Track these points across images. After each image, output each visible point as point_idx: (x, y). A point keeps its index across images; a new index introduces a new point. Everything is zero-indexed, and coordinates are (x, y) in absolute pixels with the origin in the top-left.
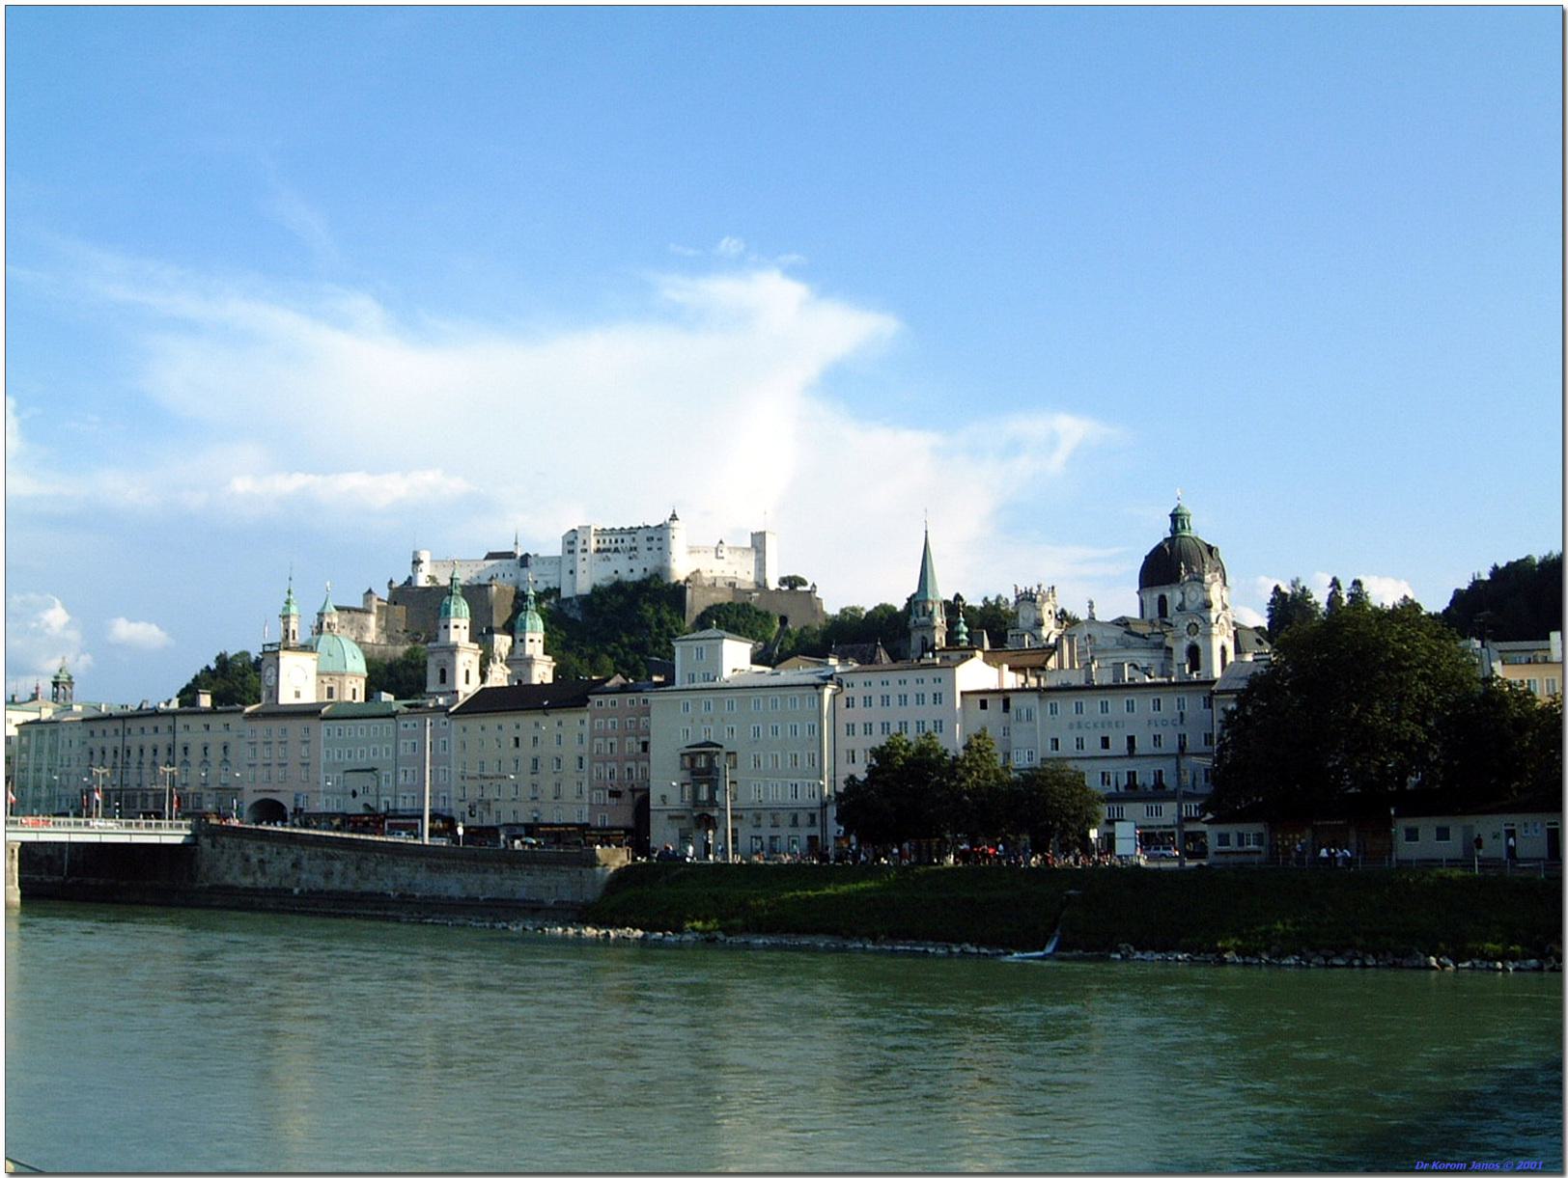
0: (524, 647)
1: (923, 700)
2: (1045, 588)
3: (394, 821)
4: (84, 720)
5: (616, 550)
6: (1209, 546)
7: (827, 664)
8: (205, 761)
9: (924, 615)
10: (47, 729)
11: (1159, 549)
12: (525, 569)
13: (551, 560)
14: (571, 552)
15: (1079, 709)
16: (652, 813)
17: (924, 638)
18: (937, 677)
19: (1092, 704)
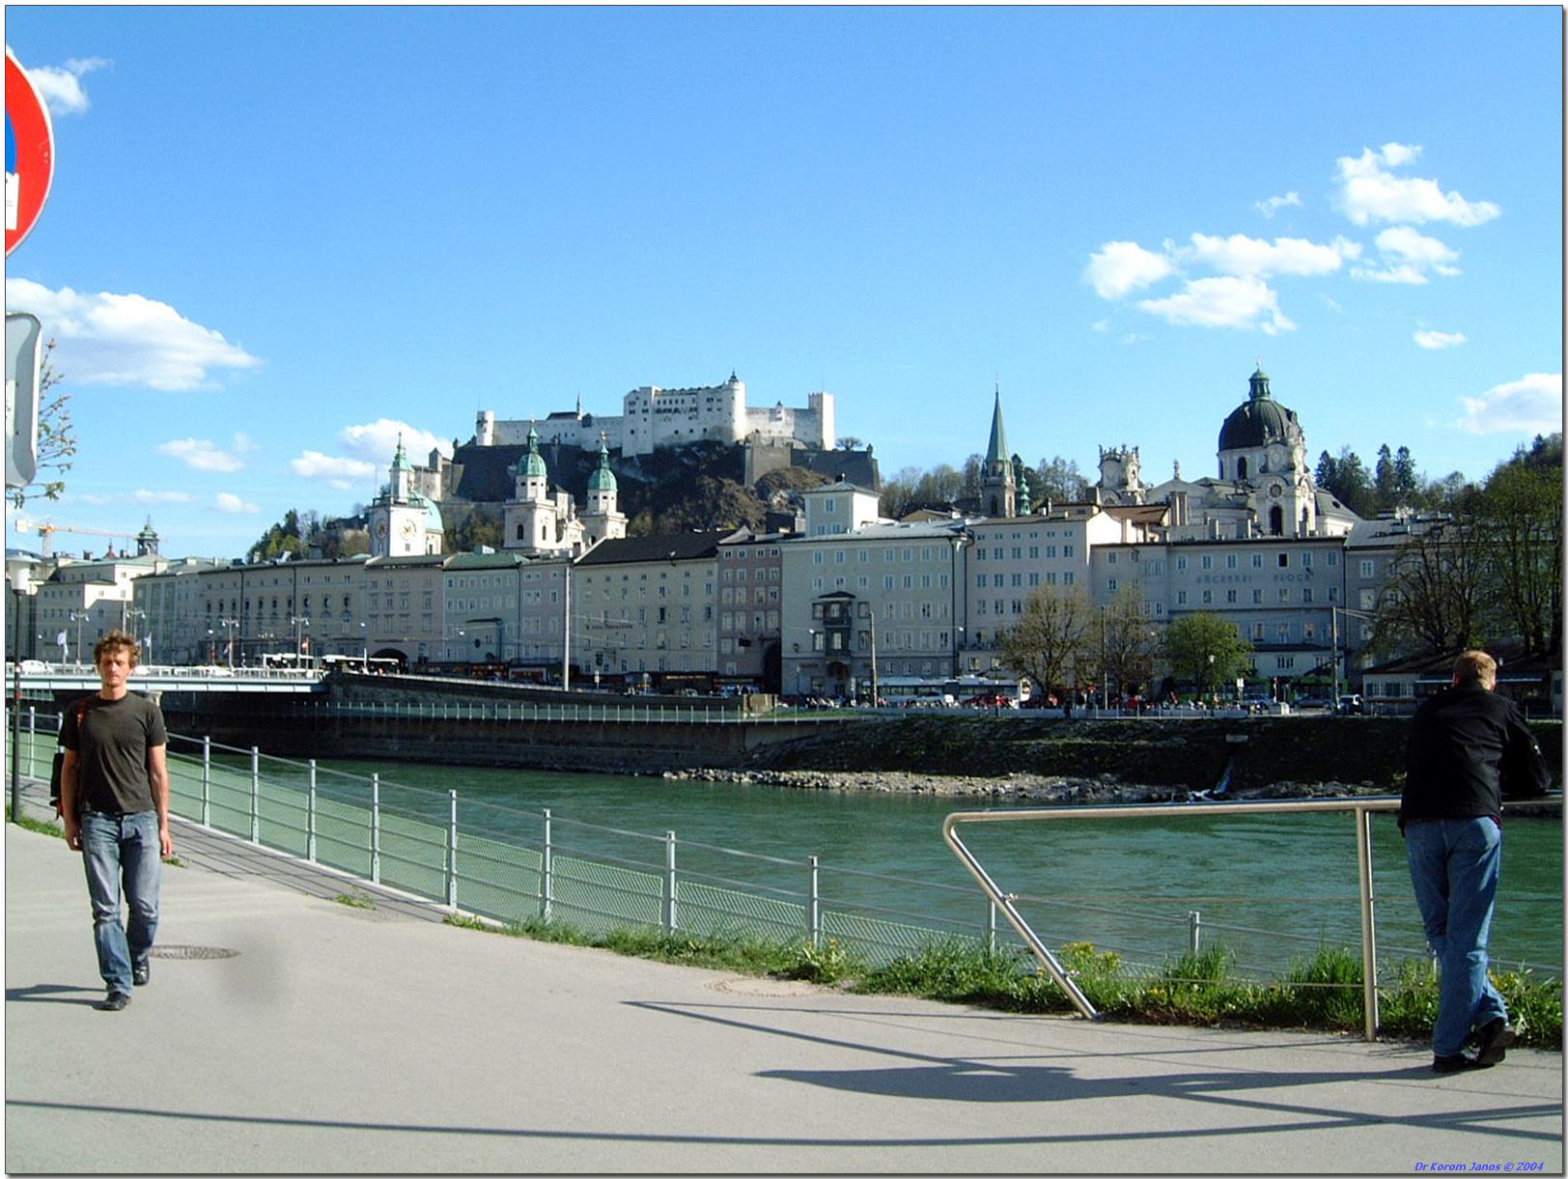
0: (598, 503)
1: (1054, 552)
2: (1129, 449)
3: (518, 670)
4: (200, 573)
5: (676, 410)
6: (1287, 410)
7: (951, 518)
8: (326, 612)
9: (994, 475)
10: (163, 582)
11: (1238, 414)
12: (587, 429)
13: (612, 420)
14: (632, 412)
15: (1207, 563)
16: (784, 662)
17: (994, 497)
18: (1068, 530)
19: (1219, 558)
